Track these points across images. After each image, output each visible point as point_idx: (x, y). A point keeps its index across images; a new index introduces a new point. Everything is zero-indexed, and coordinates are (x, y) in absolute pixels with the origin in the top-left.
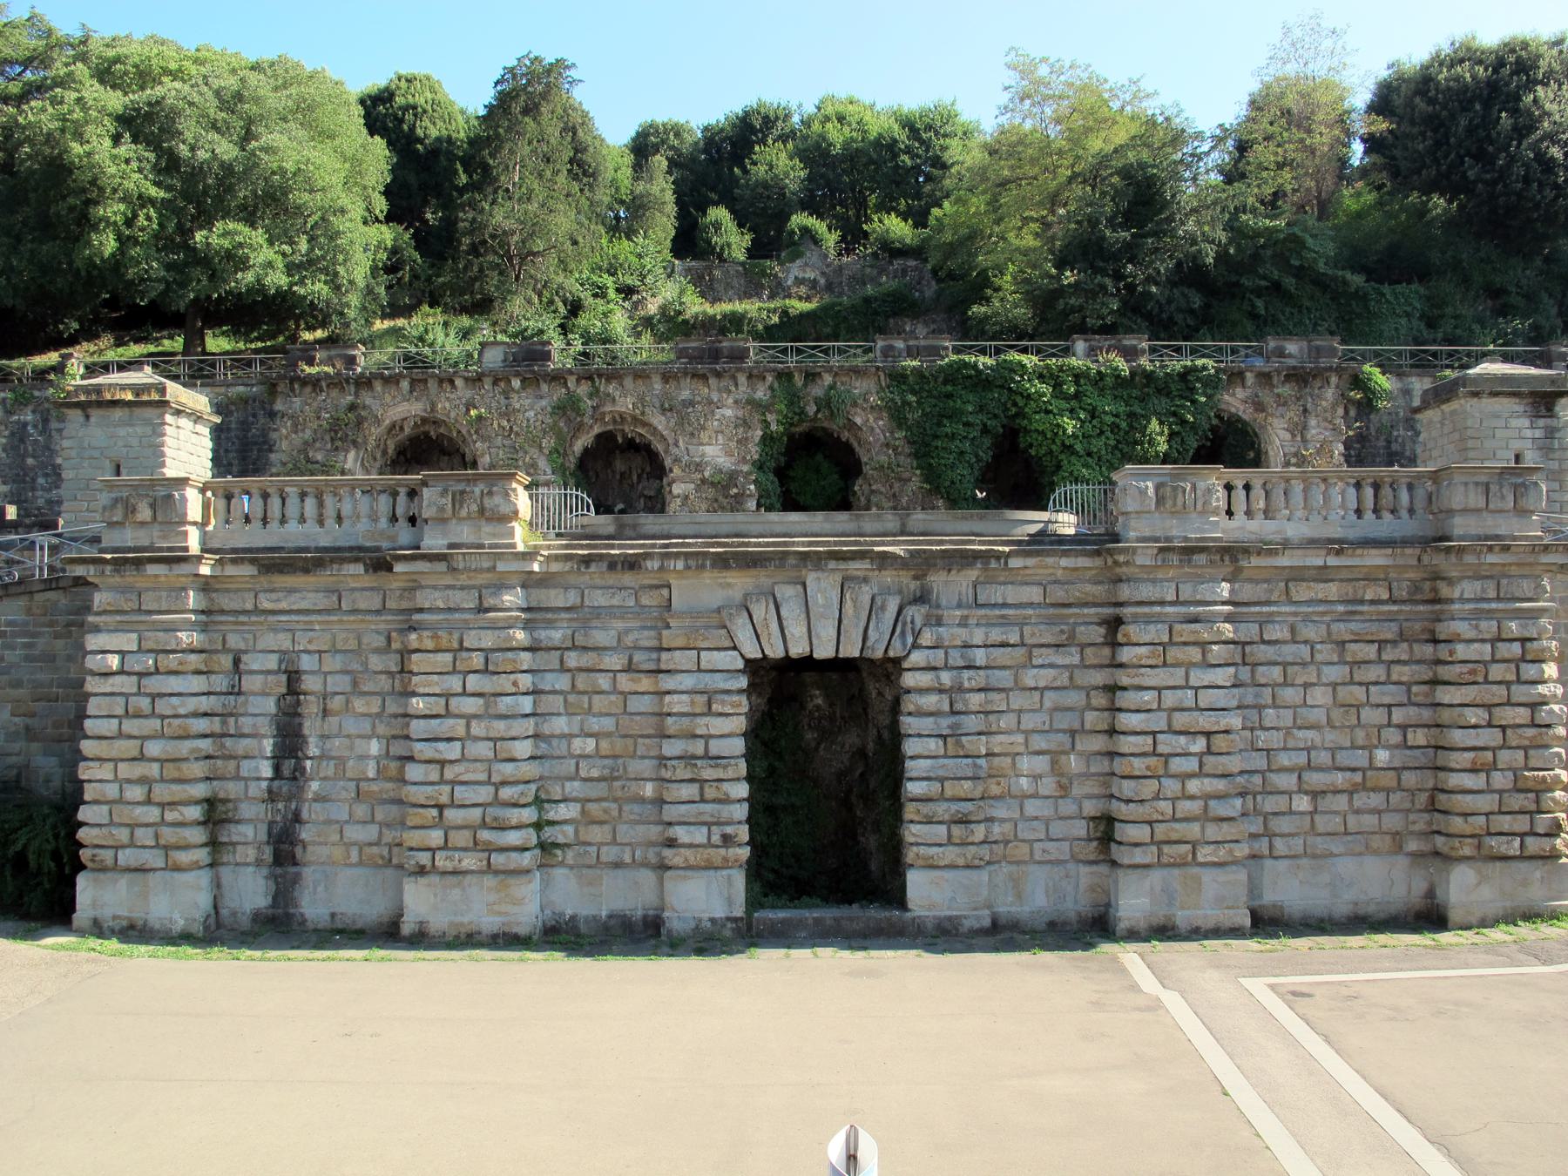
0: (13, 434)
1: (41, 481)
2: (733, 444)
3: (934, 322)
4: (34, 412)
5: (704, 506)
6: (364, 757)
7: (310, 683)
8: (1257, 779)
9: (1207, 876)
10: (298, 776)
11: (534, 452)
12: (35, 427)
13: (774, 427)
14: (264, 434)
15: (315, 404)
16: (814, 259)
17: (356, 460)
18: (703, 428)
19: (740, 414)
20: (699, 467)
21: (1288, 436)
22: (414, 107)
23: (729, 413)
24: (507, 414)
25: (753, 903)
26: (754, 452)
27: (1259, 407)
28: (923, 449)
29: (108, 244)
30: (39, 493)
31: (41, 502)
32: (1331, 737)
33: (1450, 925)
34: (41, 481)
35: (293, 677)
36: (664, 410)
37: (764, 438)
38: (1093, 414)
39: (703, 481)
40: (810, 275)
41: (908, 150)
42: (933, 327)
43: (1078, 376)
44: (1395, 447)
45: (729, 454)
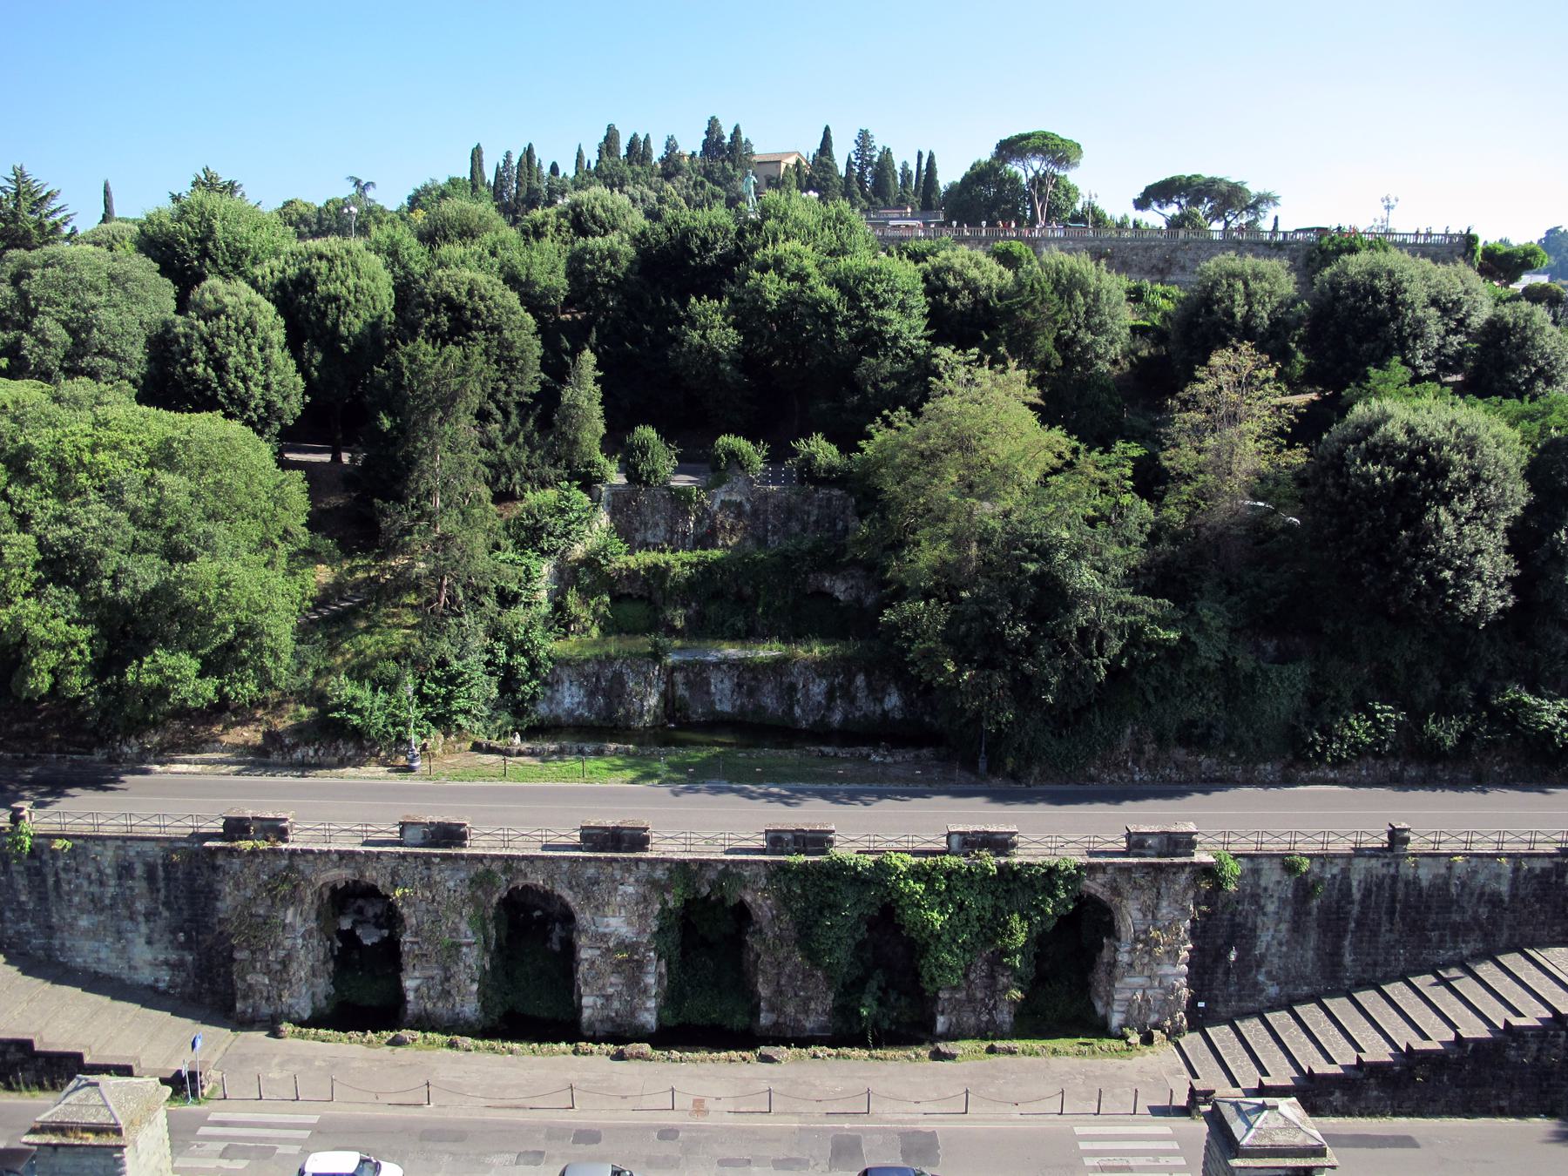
1: (8, 914)
2: (634, 919)
3: (853, 577)
5: (609, 969)
13: (671, 905)
14: (209, 885)
15: (253, 868)
16: (741, 484)
17: (295, 915)
18: (608, 904)
19: (641, 891)
21: (1140, 916)
22: (336, 298)
23: (631, 890)
24: (429, 885)
26: (654, 926)
28: (805, 934)
29: (44, 682)
31: (11, 932)
34: (8, 914)
36: (571, 888)
37: (662, 910)
38: (961, 907)
39: (608, 949)
40: (736, 498)
41: (846, 323)
42: (852, 582)
43: (950, 874)
44: (1238, 919)
45: (630, 924)
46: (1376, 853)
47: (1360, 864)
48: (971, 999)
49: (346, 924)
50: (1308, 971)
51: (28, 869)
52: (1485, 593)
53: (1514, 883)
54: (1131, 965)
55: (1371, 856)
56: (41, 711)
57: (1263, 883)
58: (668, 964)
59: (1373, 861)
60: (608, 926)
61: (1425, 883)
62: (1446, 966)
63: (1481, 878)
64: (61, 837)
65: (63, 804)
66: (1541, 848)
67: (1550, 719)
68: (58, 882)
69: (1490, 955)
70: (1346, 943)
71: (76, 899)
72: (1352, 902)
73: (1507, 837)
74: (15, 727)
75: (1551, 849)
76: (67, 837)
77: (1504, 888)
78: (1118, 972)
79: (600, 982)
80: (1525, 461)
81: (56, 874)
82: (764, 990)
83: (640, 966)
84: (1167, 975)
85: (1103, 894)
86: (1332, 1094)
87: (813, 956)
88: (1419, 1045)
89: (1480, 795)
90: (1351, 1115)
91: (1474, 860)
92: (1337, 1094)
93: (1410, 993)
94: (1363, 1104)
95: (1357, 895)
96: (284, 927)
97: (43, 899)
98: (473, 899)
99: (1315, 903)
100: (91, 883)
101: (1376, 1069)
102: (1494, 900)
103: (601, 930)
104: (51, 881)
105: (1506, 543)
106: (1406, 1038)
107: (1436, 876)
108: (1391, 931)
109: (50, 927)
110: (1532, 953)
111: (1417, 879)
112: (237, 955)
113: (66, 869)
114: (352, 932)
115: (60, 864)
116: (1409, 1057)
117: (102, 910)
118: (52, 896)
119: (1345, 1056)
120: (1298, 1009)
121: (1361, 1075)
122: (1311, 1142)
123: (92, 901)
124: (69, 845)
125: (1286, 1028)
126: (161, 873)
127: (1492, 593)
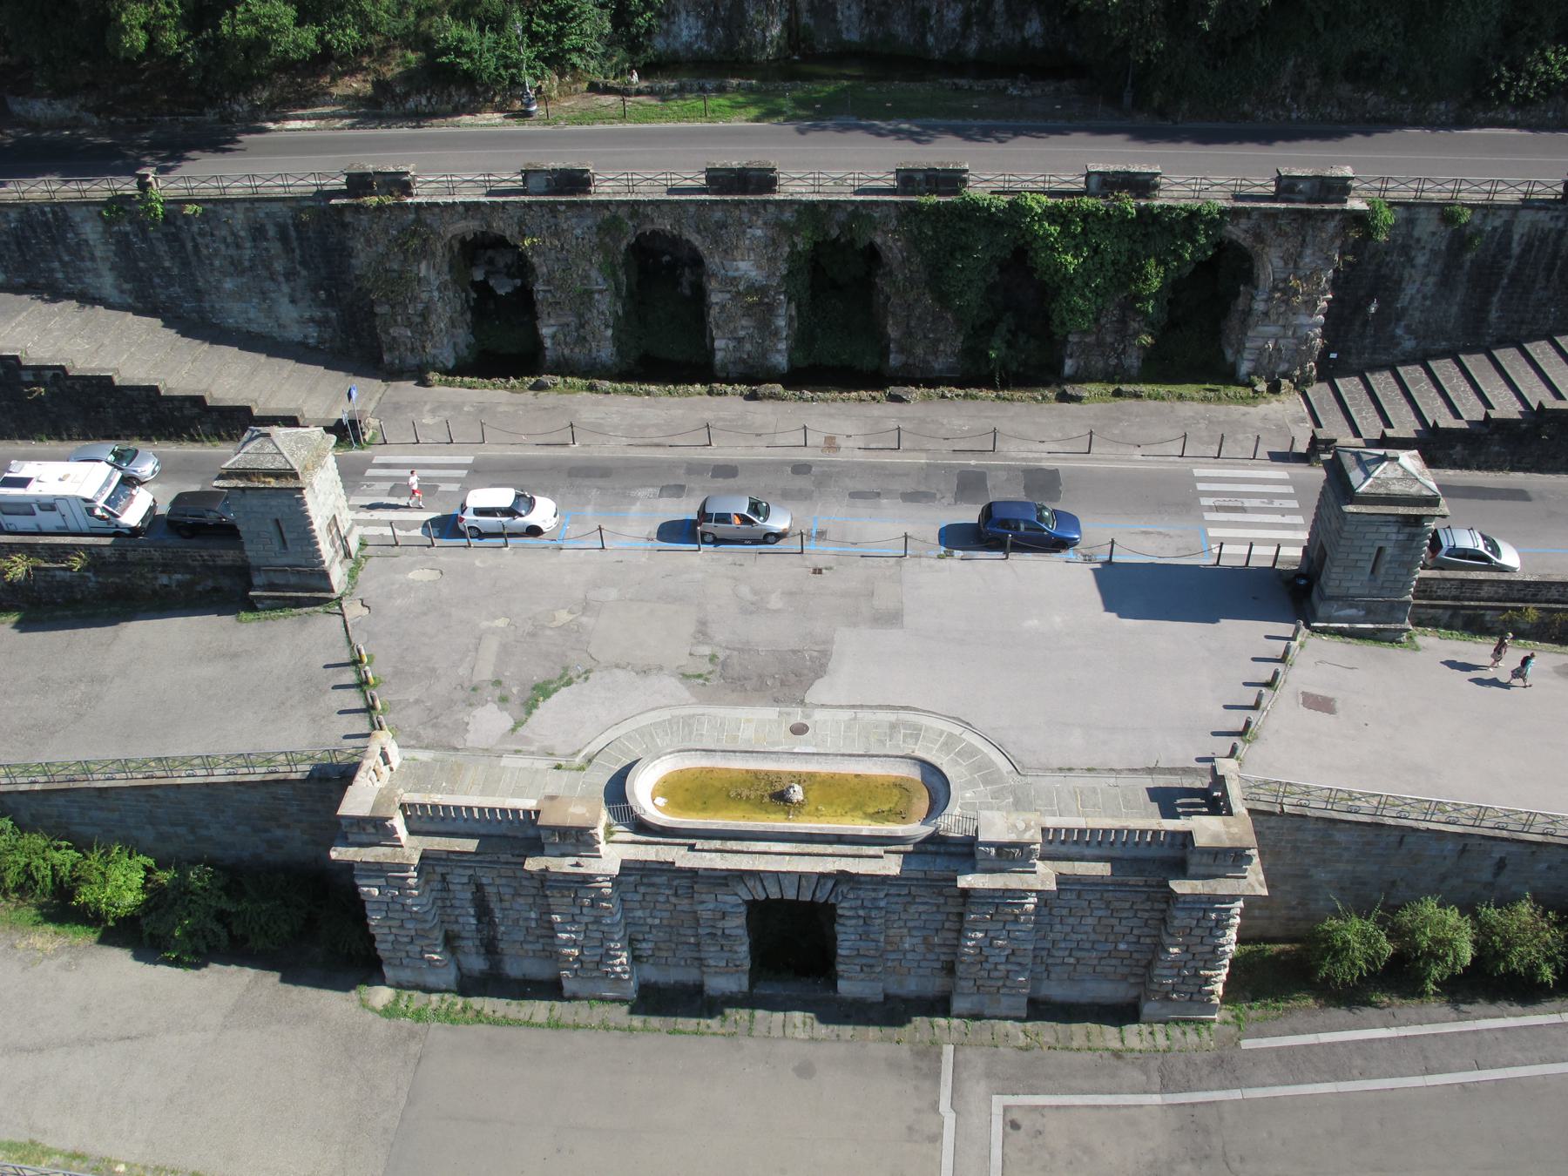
0: (118, 242)
1: (157, 280)
4: (130, 223)
6: (527, 919)
7: (490, 890)
8: (1044, 953)
9: (1003, 999)
10: (492, 924)
11: (584, 265)
12: (136, 236)
13: (800, 247)
17: (428, 269)
18: (737, 247)
20: (734, 281)
21: (1281, 264)
23: (759, 232)
24: (557, 234)
25: (752, 984)
26: (783, 269)
27: (1259, 237)
29: (140, 39)
30: (159, 290)
31: (163, 297)
32: (1093, 937)
33: (1142, 1018)
34: (157, 280)
35: (479, 887)
36: (699, 232)
37: (791, 253)
39: (738, 293)
43: (1086, 216)
44: (1384, 271)
45: (760, 267)
46: (1546, 205)
47: (1527, 216)
48: (1100, 343)
49: (479, 275)
50: (1450, 326)
51: (165, 235)
54: (1266, 314)
55: (1540, 208)
56: (143, 71)
57: (1416, 234)
58: (798, 307)
59: (1542, 214)
60: (737, 269)
64: (190, 202)
65: (186, 168)
68: (196, 246)
70: (1495, 299)
71: (217, 263)
72: (1509, 257)
74: (122, 90)
76: (197, 202)
78: (1252, 320)
79: (732, 326)
81: (193, 239)
82: (893, 332)
83: (770, 309)
84: (1302, 325)
85: (1245, 240)
86: (1453, 447)
87: (943, 299)
90: (1468, 468)
92: (1459, 448)
93: (1553, 353)
94: (1482, 459)
95: (1516, 249)
96: (419, 280)
97: (185, 264)
98: (601, 246)
99: (1469, 256)
100: (227, 246)
101: (1504, 424)
103: (730, 273)
104: (189, 246)
106: (1538, 395)
108: (1545, 288)
109: (198, 291)
112: (378, 310)
113: (202, 234)
114: (485, 282)
115: (195, 229)
116: (1538, 417)
117: (242, 273)
118: (193, 259)
119: (1472, 411)
120: (1432, 364)
121: (1486, 431)
122: (1425, 492)
123: (232, 263)
124: (200, 209)
125: (1416, 382)
126: (293, 233)
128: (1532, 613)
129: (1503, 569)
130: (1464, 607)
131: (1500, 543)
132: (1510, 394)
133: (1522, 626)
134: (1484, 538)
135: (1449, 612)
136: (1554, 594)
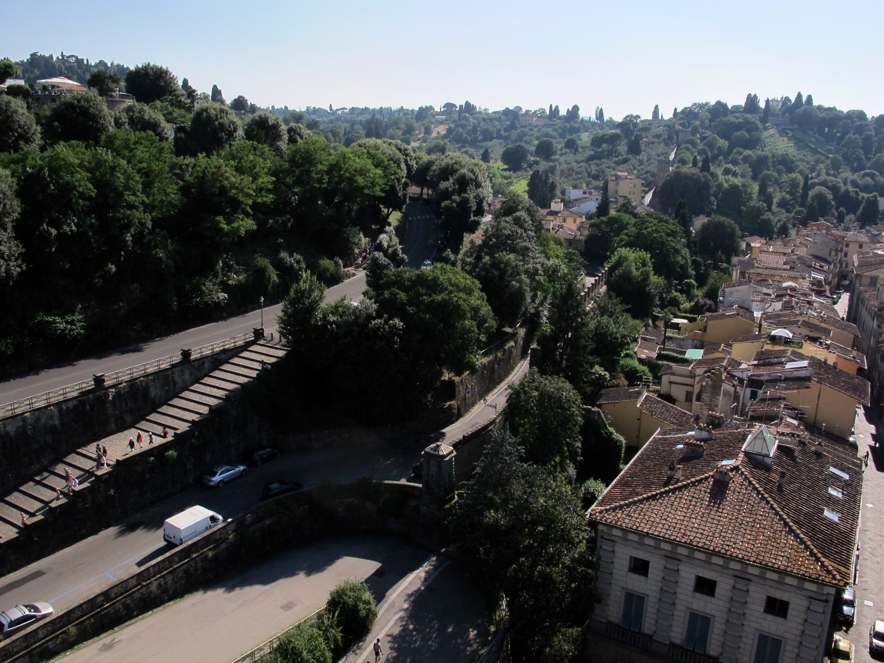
52: (8, 265)
53: (61, 418)
61: (12, 434)
62: (39, 473)
63: (43, 421)
66: (70, 396)
67: (62, 326)
69: (60, 460)
73: (51, 395)
75: (75, 394)
77: (57, 422)
80: (15, 187)
88: (30, 521)
89: (35, 376)
91: (37, 413)
93: (21, 496)
102: (53, 430)
105: (14, 235)
107: (18, 428)
110: (80, 450)
111: (7, 433)
127: (12, 264)
128: (72, 629)
129: (45, 616)
130: (33, 649)
131: (37, 605)
132: (8, 526)
133: (72, 639)
134: (26, 606)
135: (27, 657)
136: (78, 613)
